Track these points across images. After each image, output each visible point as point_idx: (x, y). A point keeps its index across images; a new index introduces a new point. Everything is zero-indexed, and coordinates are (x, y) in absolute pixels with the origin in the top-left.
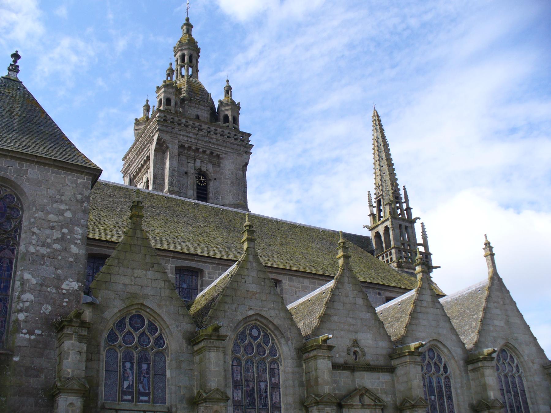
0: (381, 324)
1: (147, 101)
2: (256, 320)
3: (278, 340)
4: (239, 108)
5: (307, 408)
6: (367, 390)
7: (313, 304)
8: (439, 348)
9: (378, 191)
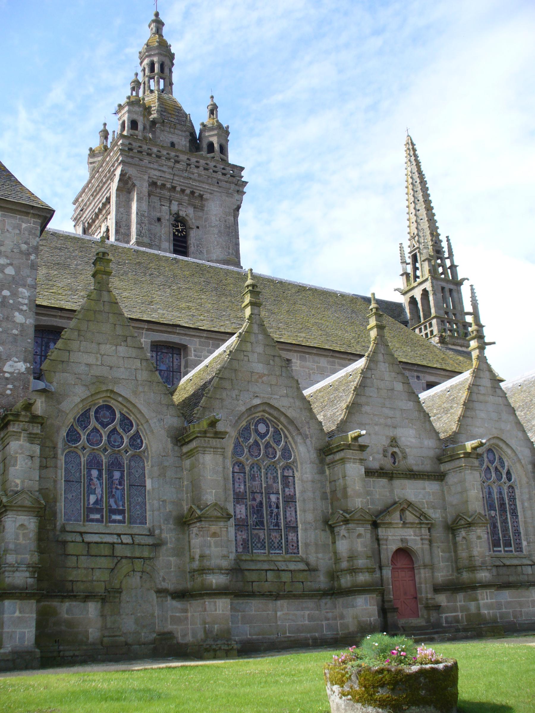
0: (427, 416)
1: (105, 125)
2: (264, 411)
3: (293, 438)
4: (228, 133)
5: (332, 528)
6: (410, 504)
7: (336, 390)
8: (501, 448)
9: (414, 242)
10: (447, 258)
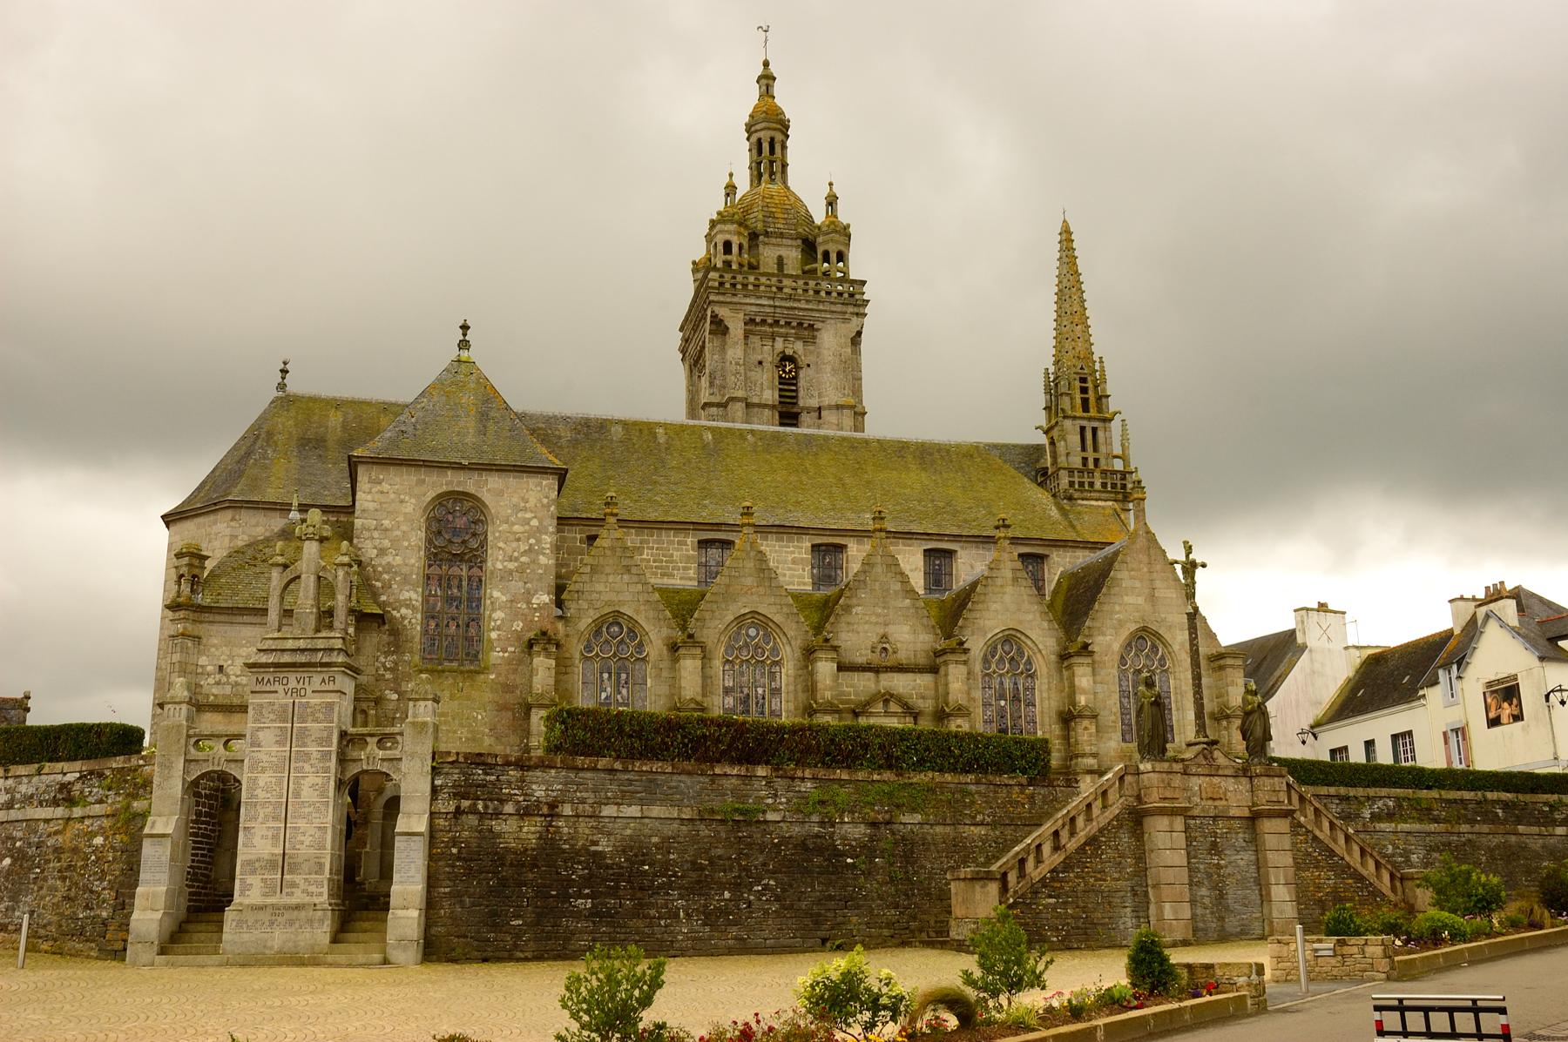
6: (892, 695)
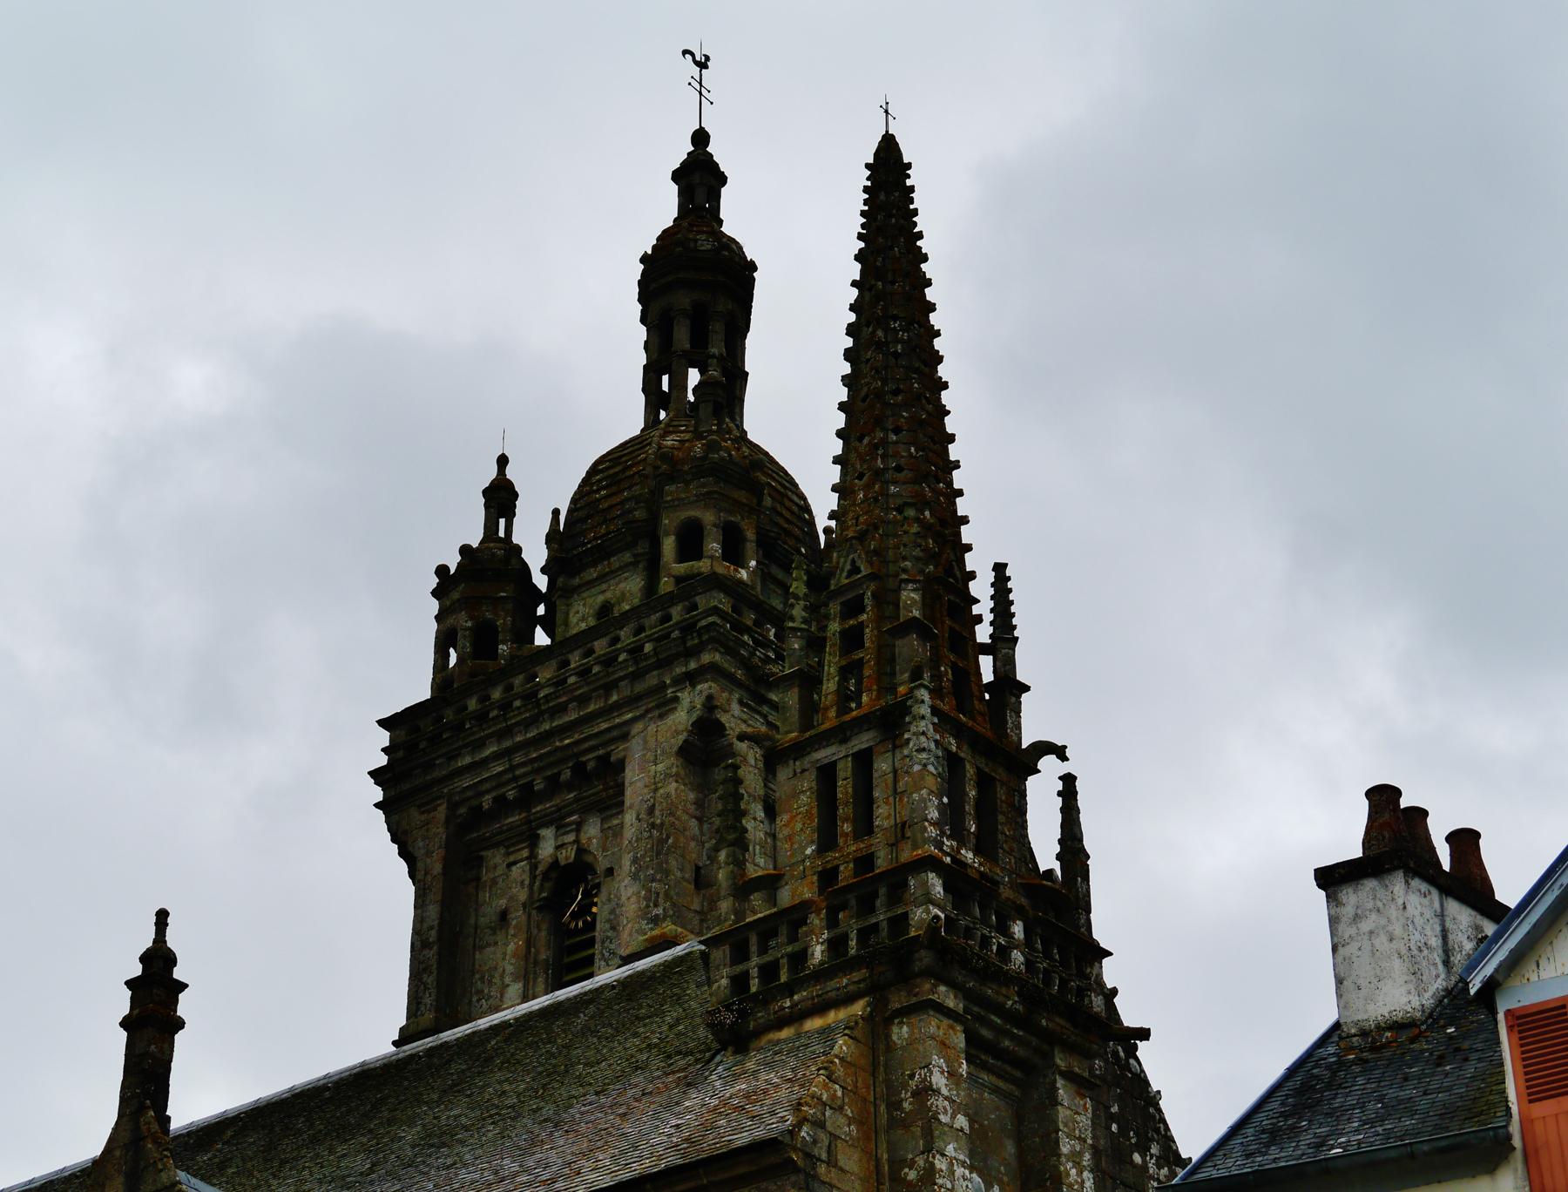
10: (984, 649)
